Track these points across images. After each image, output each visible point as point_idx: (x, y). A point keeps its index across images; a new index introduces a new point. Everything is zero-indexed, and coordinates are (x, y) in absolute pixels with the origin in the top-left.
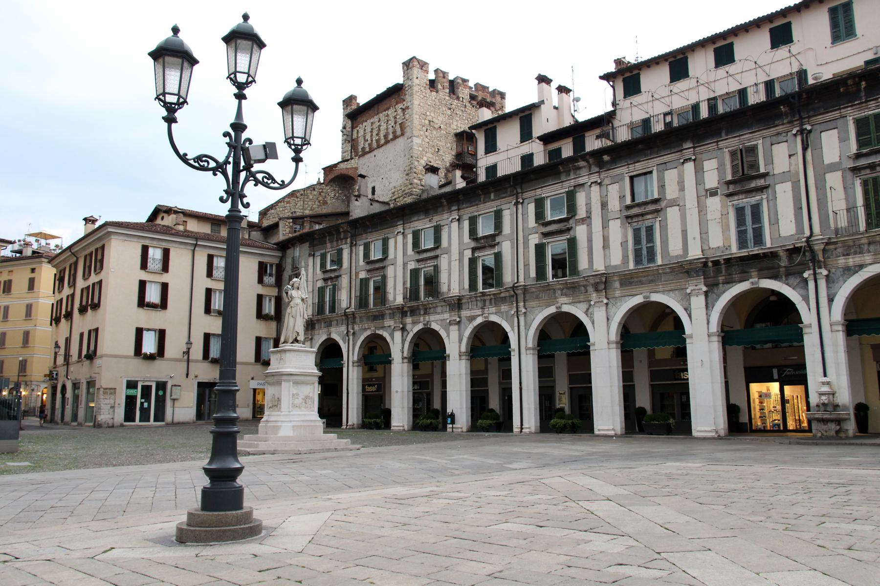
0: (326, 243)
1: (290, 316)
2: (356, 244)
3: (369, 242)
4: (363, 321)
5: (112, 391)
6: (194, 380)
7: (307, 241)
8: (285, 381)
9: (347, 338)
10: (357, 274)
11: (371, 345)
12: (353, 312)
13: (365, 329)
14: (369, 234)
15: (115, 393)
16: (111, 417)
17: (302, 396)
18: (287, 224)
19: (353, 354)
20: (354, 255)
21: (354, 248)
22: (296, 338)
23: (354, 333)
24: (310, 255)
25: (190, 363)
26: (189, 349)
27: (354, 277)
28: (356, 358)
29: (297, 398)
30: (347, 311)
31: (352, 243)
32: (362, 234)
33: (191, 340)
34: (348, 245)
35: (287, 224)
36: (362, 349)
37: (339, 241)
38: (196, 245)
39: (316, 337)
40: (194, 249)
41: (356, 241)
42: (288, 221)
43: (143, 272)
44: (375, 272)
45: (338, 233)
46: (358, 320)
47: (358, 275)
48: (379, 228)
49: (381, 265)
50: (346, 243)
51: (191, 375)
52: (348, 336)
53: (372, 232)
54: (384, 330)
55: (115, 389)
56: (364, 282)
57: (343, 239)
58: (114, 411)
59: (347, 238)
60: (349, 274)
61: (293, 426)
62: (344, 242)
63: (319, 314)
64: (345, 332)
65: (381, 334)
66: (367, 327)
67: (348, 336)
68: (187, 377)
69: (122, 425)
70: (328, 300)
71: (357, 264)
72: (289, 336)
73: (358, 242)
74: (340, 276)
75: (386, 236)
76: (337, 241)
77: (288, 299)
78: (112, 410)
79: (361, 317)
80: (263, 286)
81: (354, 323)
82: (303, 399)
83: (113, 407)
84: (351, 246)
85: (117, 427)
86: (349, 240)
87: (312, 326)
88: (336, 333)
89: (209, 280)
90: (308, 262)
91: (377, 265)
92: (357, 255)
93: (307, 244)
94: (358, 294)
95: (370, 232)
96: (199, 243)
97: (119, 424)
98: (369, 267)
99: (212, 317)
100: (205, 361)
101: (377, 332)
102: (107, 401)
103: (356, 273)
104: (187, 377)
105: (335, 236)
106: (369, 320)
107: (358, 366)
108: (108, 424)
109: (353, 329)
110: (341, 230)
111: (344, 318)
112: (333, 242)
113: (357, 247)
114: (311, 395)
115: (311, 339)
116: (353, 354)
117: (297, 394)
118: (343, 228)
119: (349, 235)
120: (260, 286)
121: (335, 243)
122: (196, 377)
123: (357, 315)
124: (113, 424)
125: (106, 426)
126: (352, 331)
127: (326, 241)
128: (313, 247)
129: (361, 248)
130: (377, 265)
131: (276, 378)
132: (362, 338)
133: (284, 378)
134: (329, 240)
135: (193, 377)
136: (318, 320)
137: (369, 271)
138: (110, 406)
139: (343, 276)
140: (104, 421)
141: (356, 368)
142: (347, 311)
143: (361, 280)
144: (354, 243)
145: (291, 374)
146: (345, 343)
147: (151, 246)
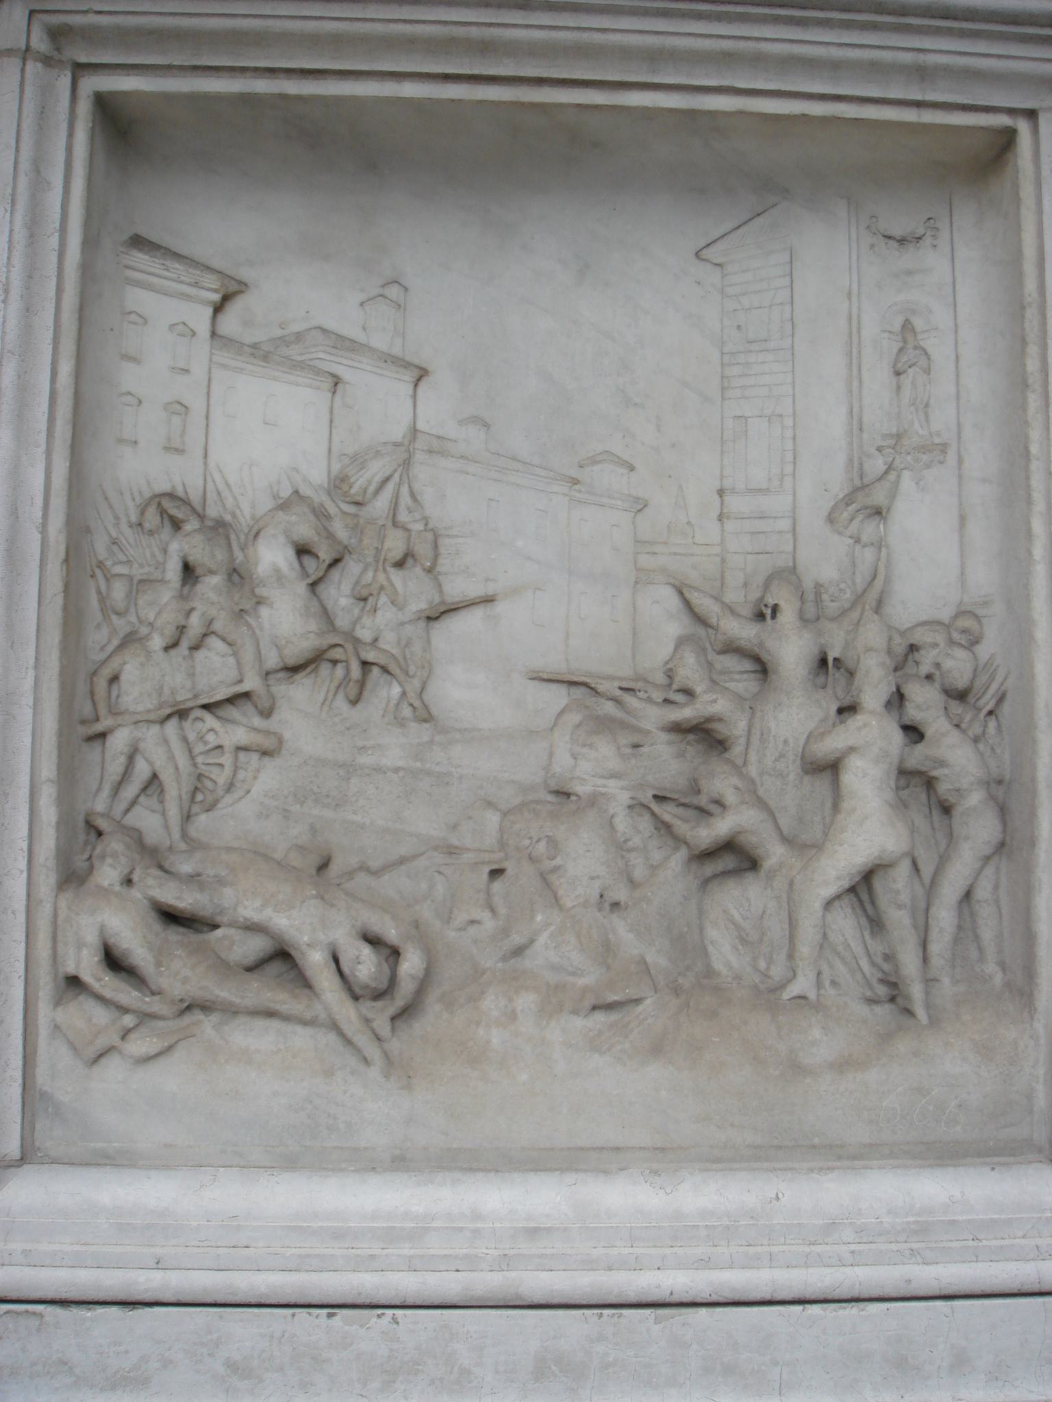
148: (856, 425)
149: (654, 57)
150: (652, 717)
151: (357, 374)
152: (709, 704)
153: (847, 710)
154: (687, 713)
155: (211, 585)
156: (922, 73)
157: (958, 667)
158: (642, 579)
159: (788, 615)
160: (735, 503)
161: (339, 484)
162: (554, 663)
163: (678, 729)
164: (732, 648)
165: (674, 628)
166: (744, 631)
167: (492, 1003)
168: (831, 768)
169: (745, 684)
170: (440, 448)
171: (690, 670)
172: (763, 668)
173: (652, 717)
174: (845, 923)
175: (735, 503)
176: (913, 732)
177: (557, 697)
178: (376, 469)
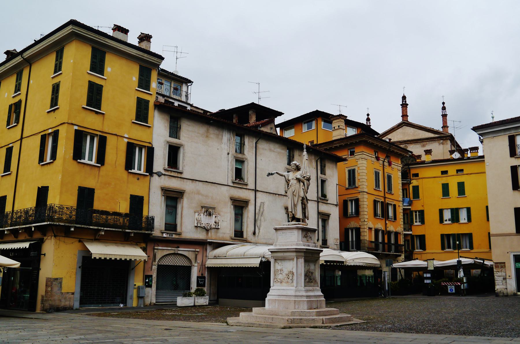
5: (503, 265)
15: (505, 267)
16: (505, 287)
17: (286, 271)
43: (513, 159)
55: (504, 263)
58: (506, 282)
69: (515, 295)
78: (504, 281)
82: (286, 275)
83: (505, 279)
85: (511, 296)
97: (512, 294)
102: (500, 274)
108: (503, 293)
124: (507, 293)
125: (501, 295)
138: (502, 277)
140: (499, 290)
147: (517, 135)
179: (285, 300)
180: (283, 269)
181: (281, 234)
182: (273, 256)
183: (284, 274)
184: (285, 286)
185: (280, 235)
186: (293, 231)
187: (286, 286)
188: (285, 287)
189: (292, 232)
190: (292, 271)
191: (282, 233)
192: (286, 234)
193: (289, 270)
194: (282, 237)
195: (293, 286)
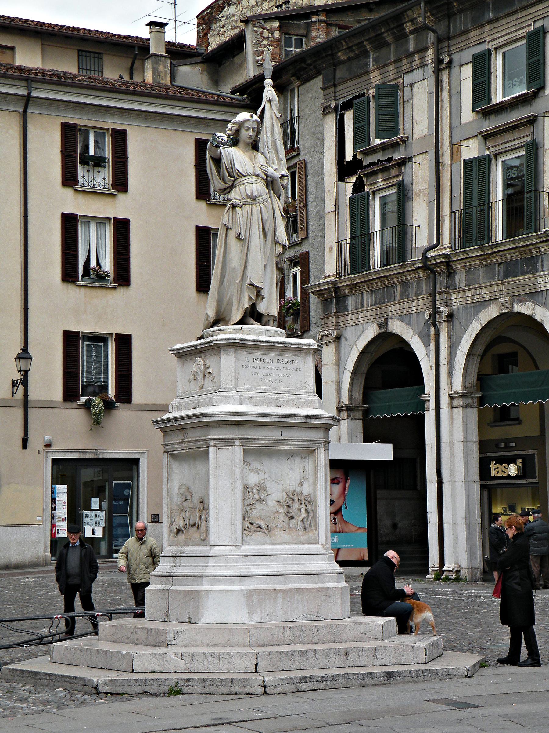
0: (367, 73)
1: (232, 235)
2: (450, 62)
3: (489, 50)
4: (475, 281)
6: (43, 453)
7: (318, 73)
8: (221, 444)
9: (432, 330)
10: (455, 148)
11: (503, 349)
12: (446, 256)
13: (483, 304)
14: (487, 28)
18: (266, 34)
19: (450, 375)
20: (445, 95)
21: (445, 76)
22: (253, 306)
23: (450, 316)
24: (326, 111)
25: (30, 411)
26: (26, 375)
27: (446, 159)
28: (458, 386)
29: (260, 500)
30: (430, 254)
31: (439, 61)
32: (467, 32)
33: (31, 351)
34: (430, 70)
35: (266, 34)
36: (476, 361)
37: (405, 61)
38: (28, 100)
39: (349, 333)
40: (25, 111)
41: (449, 55)
42: (268, 25)
44: (508, 136)
45: (402, 37)
46: (460, 279)
47: (459, 151)
48: (517, 6)
49: (523, 113)
50: (423, 65)
51: (35, 442)
52: (435, 325)
53: (496, 20)
54: (536, 303)
56: (475, 172)
57: (413, 54)
59: (426, 49)
60: (433, 153)
61: (250, 594)
62: (416, 61)
63: (354, 269)
64: (427, 315)
65: (528, 312)
66: (486, 297)
67: (435, 325)
68: (25, 446)
70: (378, 227)
71: (455, 123)
72: (230, 303)
73: (455, 57)
74: (410, 159)
75: (538, 25)
76: (398, 60)
77: (224, 180)
79: (469, 270)
80: (209, 204)
81: (450, 288)
84: (437, 71)
86: (430, 55)
87: (338, 303)
88: (401, 318)
89: (68, 192)
90: (322, 132)
91: (514, 117)
92: (454, 94)
93: (318, 82)
94: (460, 205)
95: (490, 22)
96: (34, 94)
98: (489, 125)
99: (83, 290)
100: (68, 404)
101: (518, 308)
103: (452, 145)
104: (25, 446)
105: (392, 47)
106: (492, 278)
107: (465, 407)
109: (448, 304)
110: (409, 27)
111: (421, 274)
112: (385, 66)
113: (455, 70)
114: (306, 489)
115: (338, 338)
116: (450, 375)
117: (261, 488)
118: (413, 21)
119: (431, 37)
120: (202, 205)
121: (392, 67)
122: (48, 445)
123: (457, 266)
126: (445, 311)
127: (367, 65)
128: (335, 86)
129: (467, 72)
130: (514, 117)
131: (193, 435)
132: (475, 328)
133: (214, 434)
134: (375, 60)
135: (42, 447)
136: (352, 287)
137: (487, 137)
139: (417, 159)
141: (459, 413)
142: (430, 254)
143: (467, 163)
144: (446, 60)
145: (238, 423)
146: (427, 345)
148: (300, 477)
149: (287, 445)
150: (285, 505)
151: (260, 473)
152: (290, 503)
153: (301, 504)
154: (288, 504)
155: (251, 493)
156: (309, 445)
157: (309, 499)
158: (283, 492)
159: (295, 495)
160: (290, 484)
161: (259, 483)
162: (277, 500)
163: (287, 506)
164: (291, 498)
165: (286, 496)
166: (292, 497)
167: (276, 530)
168: (300, 509)
169: (291, 501)
170: (267, 479)
171: (287, 500)
172: (293, 500)
173: (285, 505)
174: (302, 523)
175: (290, 484)
176: (306, 506)
177: (277, 503)
178: (262, 482)
179: (285, 591)
180: (268, 484)
181: (251, 363)
182: (241, 439)
183: (271, 502)
184: (286, 543)
185: (247, 367)
186: (293, 359)
187: (289, 543)
188: (287, 547)
189: (289, 362)
190: (298, 490)
191: (255, 360)
192: (268, 365)
193: (290, 489)
194: (253, 373)
195: (316, 541)
